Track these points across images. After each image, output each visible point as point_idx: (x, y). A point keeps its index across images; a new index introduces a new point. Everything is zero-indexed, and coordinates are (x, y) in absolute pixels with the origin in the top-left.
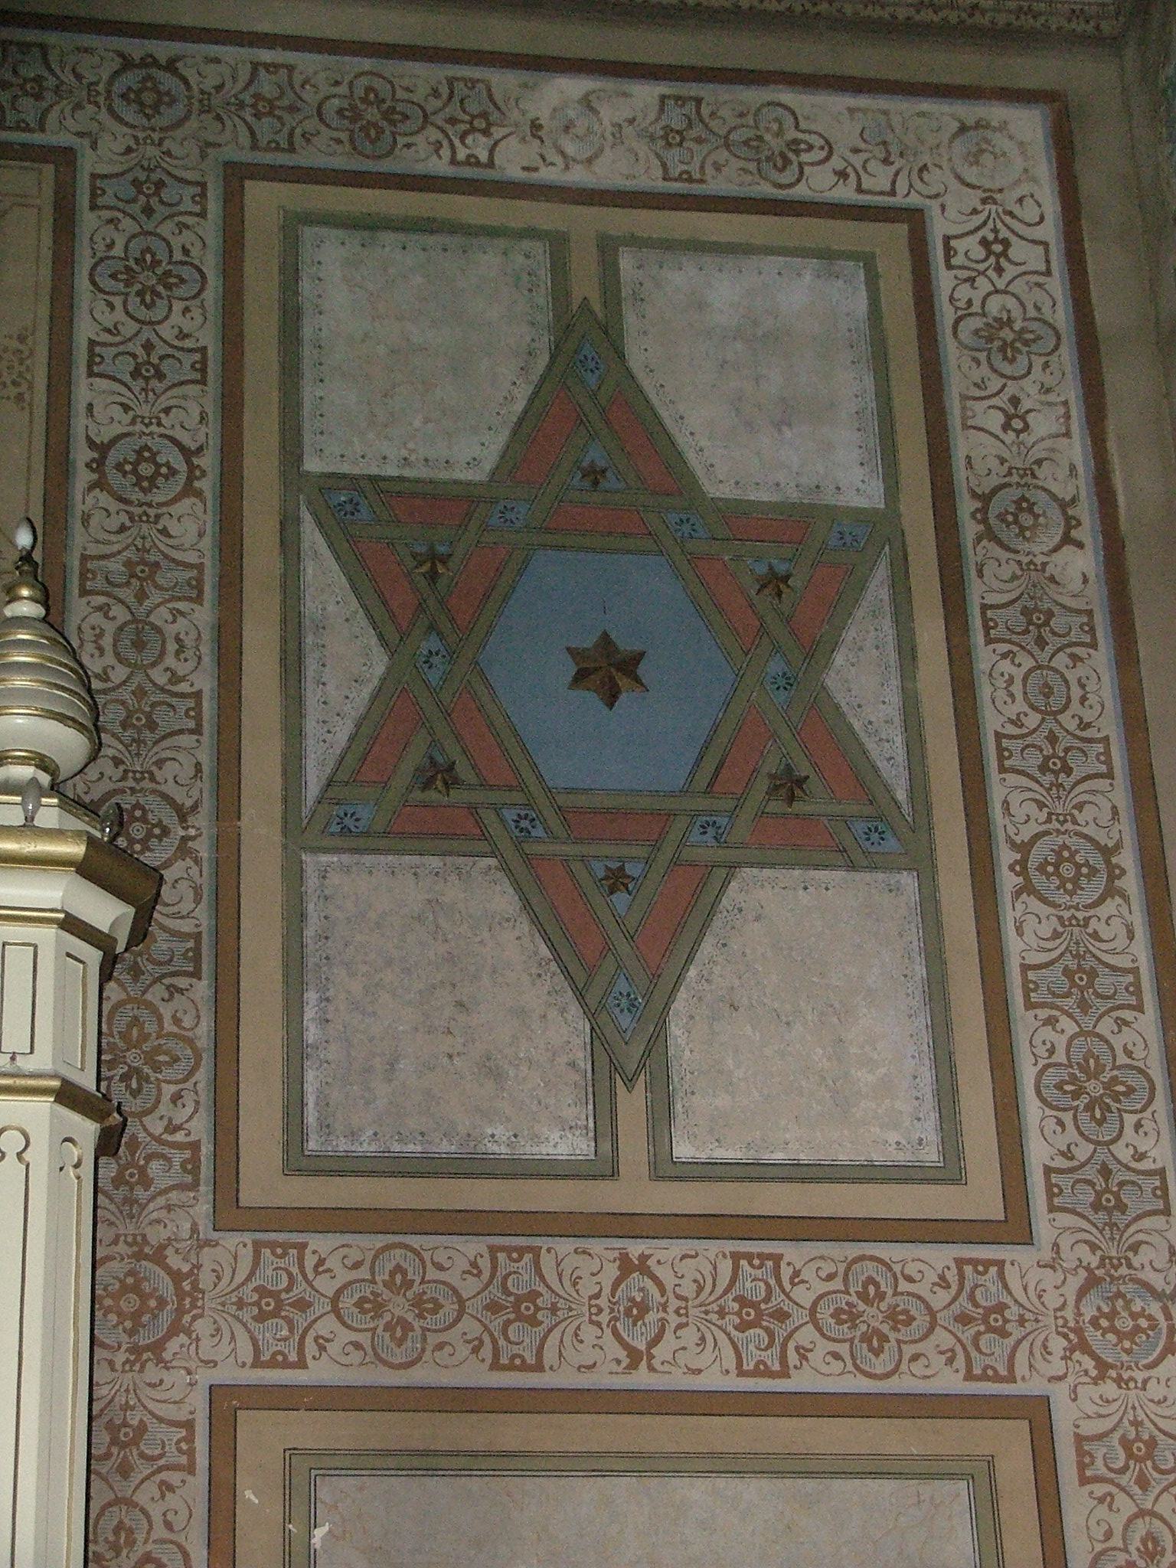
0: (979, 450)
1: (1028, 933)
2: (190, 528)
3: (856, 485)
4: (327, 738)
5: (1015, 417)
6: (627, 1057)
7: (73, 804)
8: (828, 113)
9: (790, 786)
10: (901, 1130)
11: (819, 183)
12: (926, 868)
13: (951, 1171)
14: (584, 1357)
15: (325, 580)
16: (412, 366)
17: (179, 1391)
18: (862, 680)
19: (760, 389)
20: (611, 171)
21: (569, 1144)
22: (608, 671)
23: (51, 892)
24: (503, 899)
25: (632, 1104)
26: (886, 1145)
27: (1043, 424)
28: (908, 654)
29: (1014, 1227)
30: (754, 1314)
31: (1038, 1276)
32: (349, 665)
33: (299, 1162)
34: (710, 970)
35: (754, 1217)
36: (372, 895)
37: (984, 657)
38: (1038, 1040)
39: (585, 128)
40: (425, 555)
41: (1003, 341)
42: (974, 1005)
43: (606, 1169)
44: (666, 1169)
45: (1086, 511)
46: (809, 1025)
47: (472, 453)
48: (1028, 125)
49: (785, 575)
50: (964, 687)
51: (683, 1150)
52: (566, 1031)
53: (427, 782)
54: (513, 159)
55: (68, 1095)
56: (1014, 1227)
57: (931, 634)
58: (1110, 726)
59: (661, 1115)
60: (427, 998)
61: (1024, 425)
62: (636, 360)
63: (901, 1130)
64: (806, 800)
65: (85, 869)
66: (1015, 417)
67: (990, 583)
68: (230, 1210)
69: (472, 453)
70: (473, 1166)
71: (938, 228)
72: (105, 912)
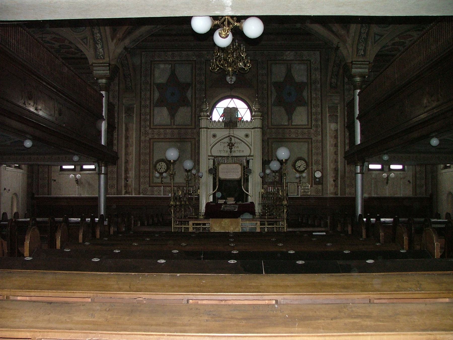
0: (313, 77)
1: (314, 110)
6: (290, 119)
7: (260, 112)
8: (305, 53)
10: (305, 122)
11: (304, 58)
13: (308, 125)
14: (287, 136)
15: (273, 88)
16: (279, 73)
17: (266, 138)
18: (305, 94)
19: (300, 74)
20: (292, 58)
21: (286, 124)
22: (290, 94)
23: (259, 118)
26: (304, 123)
28: (308, 93)
29: (311, 128)
33: (272, 125)
34: (295, 113)
35: (297, 127)
36: (276, 109)
37: (312, 92)
38: (314, 117)
39: (289, 55)
40: (279, 86)
42: (310, 114)
43: (289, 125)
44: (292, 125)
46: (300, 117)
47: (282, 80)
48: (318, 53)
49: (300, 87)
51: (293, 124)
52: (286, 117)
53: (280, 102)
54: (285, 58)
55: (260, 128)
56: (311, 128)
59: (292, 122)
60: (279, 116)
61: (317, 75)
62: (292, 72)
63: (305, 122)
64: (301, 102)
65: (261, 116)
66: (316, 75)
67: (313, 87)
68: (268, 128)
70: (281, 125)
71: (312, 61)
72: (261, 118)
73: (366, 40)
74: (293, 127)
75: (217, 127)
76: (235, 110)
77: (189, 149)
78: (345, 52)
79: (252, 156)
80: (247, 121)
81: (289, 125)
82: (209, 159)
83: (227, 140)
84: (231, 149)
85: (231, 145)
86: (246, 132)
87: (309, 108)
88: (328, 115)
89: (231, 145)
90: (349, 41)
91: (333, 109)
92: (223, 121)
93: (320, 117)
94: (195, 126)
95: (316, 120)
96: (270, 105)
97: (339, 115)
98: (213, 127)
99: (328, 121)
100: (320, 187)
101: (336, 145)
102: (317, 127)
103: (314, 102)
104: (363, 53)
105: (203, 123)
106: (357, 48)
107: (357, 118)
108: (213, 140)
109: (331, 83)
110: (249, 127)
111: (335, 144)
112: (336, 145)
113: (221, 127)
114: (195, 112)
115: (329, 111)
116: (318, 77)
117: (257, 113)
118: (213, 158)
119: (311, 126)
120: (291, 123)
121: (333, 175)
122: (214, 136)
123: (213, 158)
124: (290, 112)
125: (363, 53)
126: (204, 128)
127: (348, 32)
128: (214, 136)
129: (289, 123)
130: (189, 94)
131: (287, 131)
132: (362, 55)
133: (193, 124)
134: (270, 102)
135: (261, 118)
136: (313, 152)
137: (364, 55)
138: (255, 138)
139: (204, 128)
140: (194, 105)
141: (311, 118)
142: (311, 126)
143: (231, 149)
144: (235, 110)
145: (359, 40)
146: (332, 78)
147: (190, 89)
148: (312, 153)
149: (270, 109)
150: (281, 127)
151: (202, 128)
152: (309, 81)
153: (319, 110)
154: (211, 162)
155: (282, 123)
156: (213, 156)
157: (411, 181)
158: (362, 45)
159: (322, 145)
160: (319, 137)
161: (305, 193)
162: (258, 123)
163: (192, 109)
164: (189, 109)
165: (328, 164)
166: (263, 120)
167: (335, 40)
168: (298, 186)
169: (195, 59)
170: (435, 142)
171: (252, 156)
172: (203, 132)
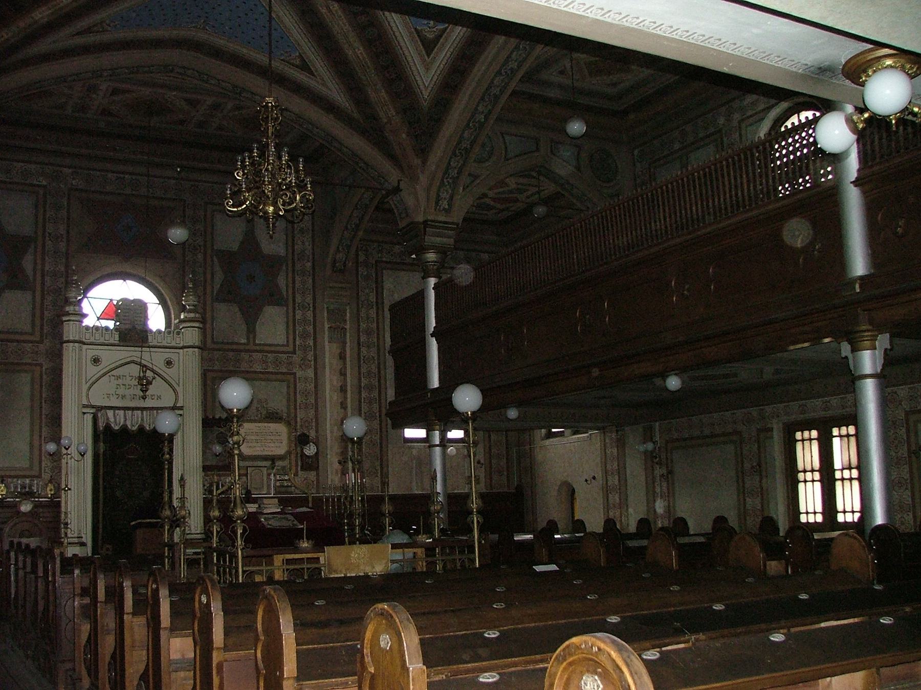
2: (200, 257)
3: (282, 252)
4: (217, 286)
5: (303, 243)
6: (251, 331)
9: (272, 295)
10: (280, 339)
12: (287, 306)
18: (282, 281)
21: (243, 341)
22: (251, 278)
23: (197, 325)
24: (237, 309)
25: (251, 336)
27: (307, 244)
28: (287, 277)
30: (265, 362)
31: (296, 358)
32: (219, 277)
33: (214, 342)
35: (266, 349)
36: (222, 308)
38: (299, 329)
40: (228, 259)
41: (302, 231)
42: (291, 324)
43: (248, 344)
44: (256, 345)
45: (311, 257)
46: (273, 327)
47: (235, 247)
49: (273, 264)
50: (294, 282)
51: (257, 342)
52: (244, 327)
53: (228, 294)
57: (290, 275)
58: (311, 287)
61: (304, 244)
63: (280, 339)
64: (274, 297)
66: (303, 243)
67: (298, 267)
69: (235, 247)
72: (201, 326)
73: (456, 180)
74: (258, 348)
75: (102, 340)
76: (139, 308)
77: (27, 389)
78: (410, 201)
79: (181, 408)
80: (159, 332)
81: (248, 344)
82: (84, 413)
83: (135, 370)
84: (144, 391)
85: (144, 384)
86: (167, 356)
87: (291, 307)
88: (327, 326)
89: (144, 384)
90: (423, 179)
91: (336, 315)
92: (116, 329)
93: (310, 329)
94: (42, 336)
95: (305, 336)
96: (209, 298)
97: (348, 327)
98: (92, 340)
99: (326, 339)
100: (312, 475)
101: (343, 389)
102: (305, 349)
103: (299, 299)
104: (447, 207)
105: (70, 331)
106: (438, 196)
107: (432, 335)
108: (93, 371)
109: (334, 262)
110: (173, 344)
111: (341, 386)
112: (343, 389)
113: (112, 341)
114: (42, 304)
115: (328, 319)
116: (308, 246)
117: (192, 315)
118: (93, 411)
119: (295, 346)
120: (254, 341)
121: (339, 451)
122: (96, 361)
123: (93, 411)
124: (251, 317)
125: (447, 207)
126: (74, 342)
127: (424, 163)
128: (96, 361)
129: (248, 339)
130: (27, 263)
131: (246, 356)
132: (444, 209)
133: (38, 334)
134: (208, 291)
135: (201, 326)
136: (299, 401)
137: (447, 211)
138: (188, 366)
139: (74, 342)
140: (38, 288)
141: (294, 332)
142: (295, 346)
143: (144, 391)
144: (139, 308)
145: (442, 180)
146: (338, 250)
147: (31, 250)
148: (295, 405)
149: (208, 308)
150: (234, 347)
151: (68, 342)
152: (290, 256)
153: (310, 314)
154: (89, 418)
155: (236, 340)
156: (93, 407)
157: (482, 461)
158: (447, 192)
159: (316, 387)
160: (310, 373)
161: (283, 489)
162: (192, 335)
163: (34, 297)
164: (28, 296)
165: (328, 426)
166: (203, 331)
167: (393, 175)
168: (269, 475)
169: (44, 183)
170: (674, 383)
171: (181, 408)
172: (70, 353)
